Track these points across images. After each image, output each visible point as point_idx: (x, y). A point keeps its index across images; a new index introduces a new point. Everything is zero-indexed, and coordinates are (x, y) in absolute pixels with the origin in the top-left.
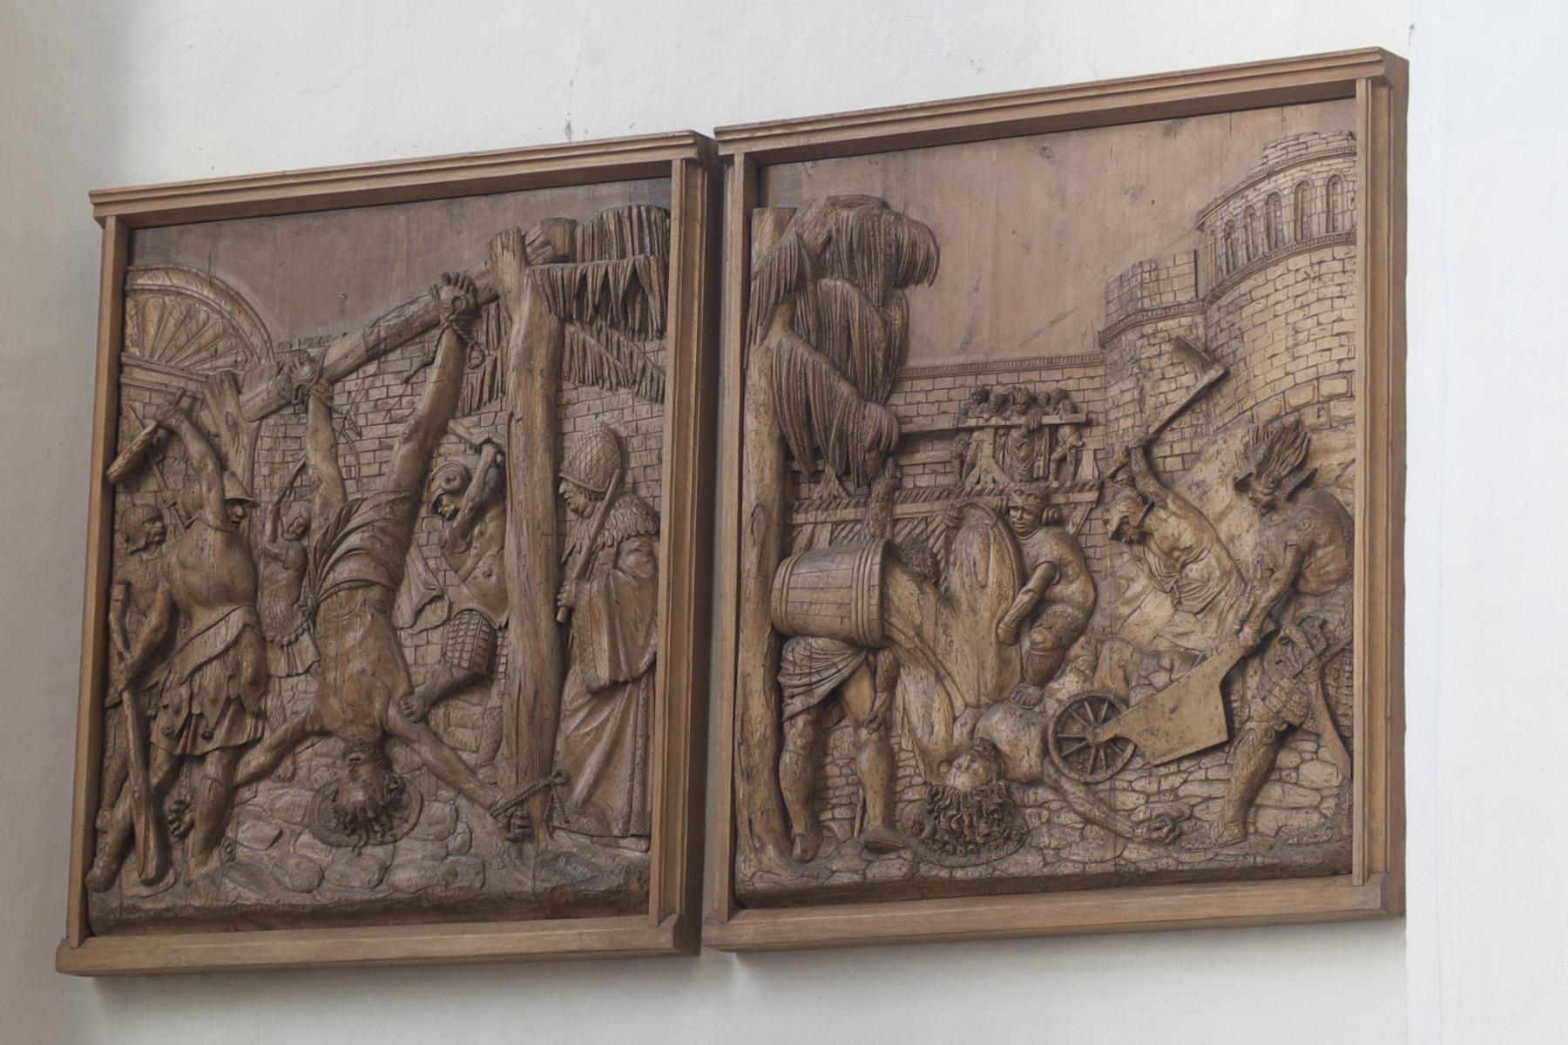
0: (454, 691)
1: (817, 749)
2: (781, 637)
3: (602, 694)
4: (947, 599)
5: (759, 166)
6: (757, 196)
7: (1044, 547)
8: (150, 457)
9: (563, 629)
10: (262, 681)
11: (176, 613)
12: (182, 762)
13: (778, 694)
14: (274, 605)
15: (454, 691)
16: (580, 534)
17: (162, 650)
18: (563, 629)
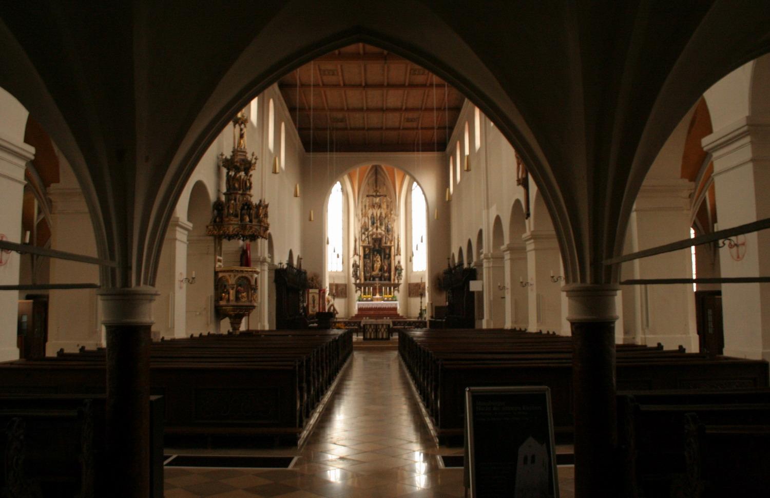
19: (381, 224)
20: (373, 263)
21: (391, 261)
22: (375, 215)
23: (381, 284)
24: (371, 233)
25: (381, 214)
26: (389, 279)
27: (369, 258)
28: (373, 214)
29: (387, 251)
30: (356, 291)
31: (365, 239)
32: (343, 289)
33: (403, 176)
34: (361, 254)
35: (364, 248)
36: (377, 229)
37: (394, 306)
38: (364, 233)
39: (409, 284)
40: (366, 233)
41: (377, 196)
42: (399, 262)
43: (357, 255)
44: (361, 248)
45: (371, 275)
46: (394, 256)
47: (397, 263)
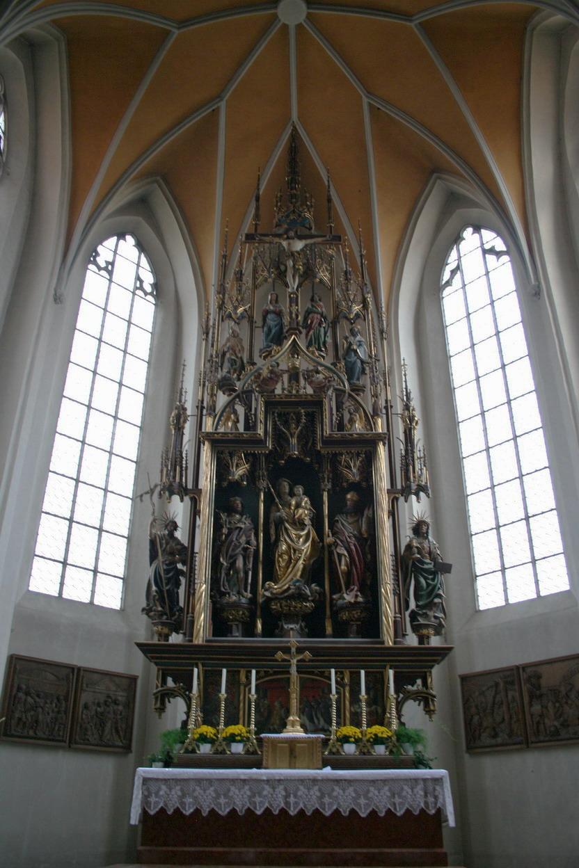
0: (500, 723)
1: (538, 727)
2: (532, 715)
3: (515, 722)
4: (548, 711)
5: (523, 668)
7: (557, 705)
9: (511, 716)
11: (472, 716)
13: (533, 721)
15: (500, 723)
16: (511, 706)
17: (471, 720)
18: (511, 716)
20: (274, 530)
21: (373, 524)
23: (315, 651)
29: (353, 474)
32: (110, 701)
33: (407, 224)
34: (207, 482)
35: (223, 447)
37: (415, 801)
39: (464, 678)
43: (183, 491)
45: (253, 600)
47: (406, 535)
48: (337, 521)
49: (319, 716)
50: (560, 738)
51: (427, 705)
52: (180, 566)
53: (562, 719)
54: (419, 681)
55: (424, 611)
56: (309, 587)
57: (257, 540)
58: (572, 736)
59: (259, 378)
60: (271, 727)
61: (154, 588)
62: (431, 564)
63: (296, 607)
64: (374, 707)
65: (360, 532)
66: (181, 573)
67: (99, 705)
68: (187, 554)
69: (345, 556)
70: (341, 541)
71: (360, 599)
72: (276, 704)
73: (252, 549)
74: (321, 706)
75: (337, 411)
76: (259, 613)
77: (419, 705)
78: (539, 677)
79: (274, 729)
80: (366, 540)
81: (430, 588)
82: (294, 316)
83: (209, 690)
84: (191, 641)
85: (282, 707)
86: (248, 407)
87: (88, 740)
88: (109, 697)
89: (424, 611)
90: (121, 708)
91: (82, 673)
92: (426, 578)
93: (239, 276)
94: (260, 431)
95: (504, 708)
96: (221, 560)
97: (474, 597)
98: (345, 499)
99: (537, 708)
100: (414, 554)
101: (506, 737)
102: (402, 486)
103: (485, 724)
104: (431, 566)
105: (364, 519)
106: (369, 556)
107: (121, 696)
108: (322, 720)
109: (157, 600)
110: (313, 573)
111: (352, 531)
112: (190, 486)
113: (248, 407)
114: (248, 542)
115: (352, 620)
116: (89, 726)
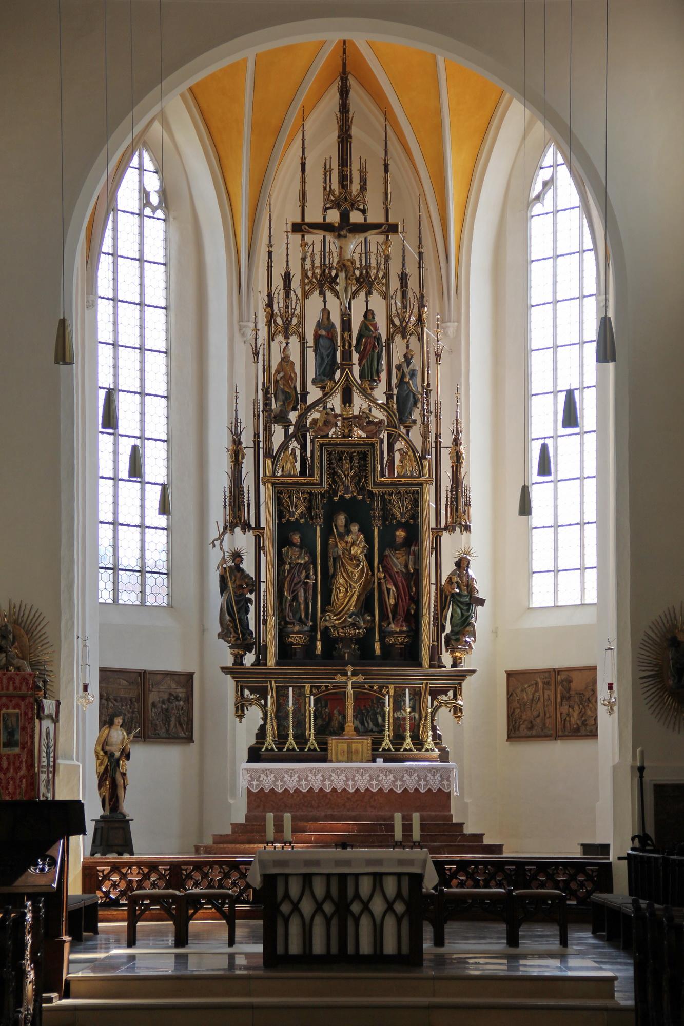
2: (561, 714)
5: (558, 672)
6: (558, 675)
8: (512, 694)
10: (521, 716)
11: (514, 710)
12: (515, 723)
13: (561, 719)
14: (522, 708)
16: (546, 704)
17: (513, 712)
19: (370, 375)
22: (336, 319)
24: (315, 415)
25: (369, 315)
26: (411, 655)
27: (307, 546)
28: (325, 323)
29: (399, 511)
30: (240, 709)
31: (284, 446)
34: (267, 518)
36: (347, 399)
38: (281, 418)
40: (293, 416)
41: (345, 228)
42: (462, 564)
43: (246, 526)
44: (265, 491)
45: (314, 628)
46: (437, 533)
47: (448, 568)
48: (386, 556)
49: (369, 721)
50: (579, 734)
51: (455, 712)
52: (248, 596)
53: (583, 719)
54: (451, 693)
55: (457, 637)
56: (363, 616)
57: (315, 573)
58: (588, 733)
59: (316, 425)
60: (332, 729)
61: (228, 618)
62: (468, 596)
63: (350, 634)
64: (413, 713)
65: (406, 566)
66: (250, 600)
67: (163, 703)
68: (254, 585)
69: (393, 591)
70: (390, 576)
71: (405, 629)
72: (335, 711)
73: (311, 582)
74: (370, 713)
75: (389, 455)
76: (319, 637)
77: (450, 711)
78: (570, 681)
79: (334, 731)
80: (412, 574)
81: (465, 617)
82: (347, 347)
83: (281, 701)
84: (266, 664)
85: (340, 714)
86: (303, 448)
87: (158, 734)
88: (171, 694)
89: (457, 637)
90: (182, 703)
91: (147, 676)
92: (461, 609)
93: (287, 278)
94: (317, 477)
95: (540, 705)
96: (286, 593)
97: (529, 594)
98: (394, 536)
99: (565, 709)
100: (454, 589)
101: (540, 730)
102: (446, 523)
103: (524, 717)
104: (467, 599)
105: (410, 557)
106: (414, 589)
107: (181, 693)
108: (371, 724)
109: (232, 627)
110: (366, 605)
111: (399, 567)
112: (253, 524)
113: (303, 448)
114: (307, 577)
115: (397, 645)
116: (157, 723)
